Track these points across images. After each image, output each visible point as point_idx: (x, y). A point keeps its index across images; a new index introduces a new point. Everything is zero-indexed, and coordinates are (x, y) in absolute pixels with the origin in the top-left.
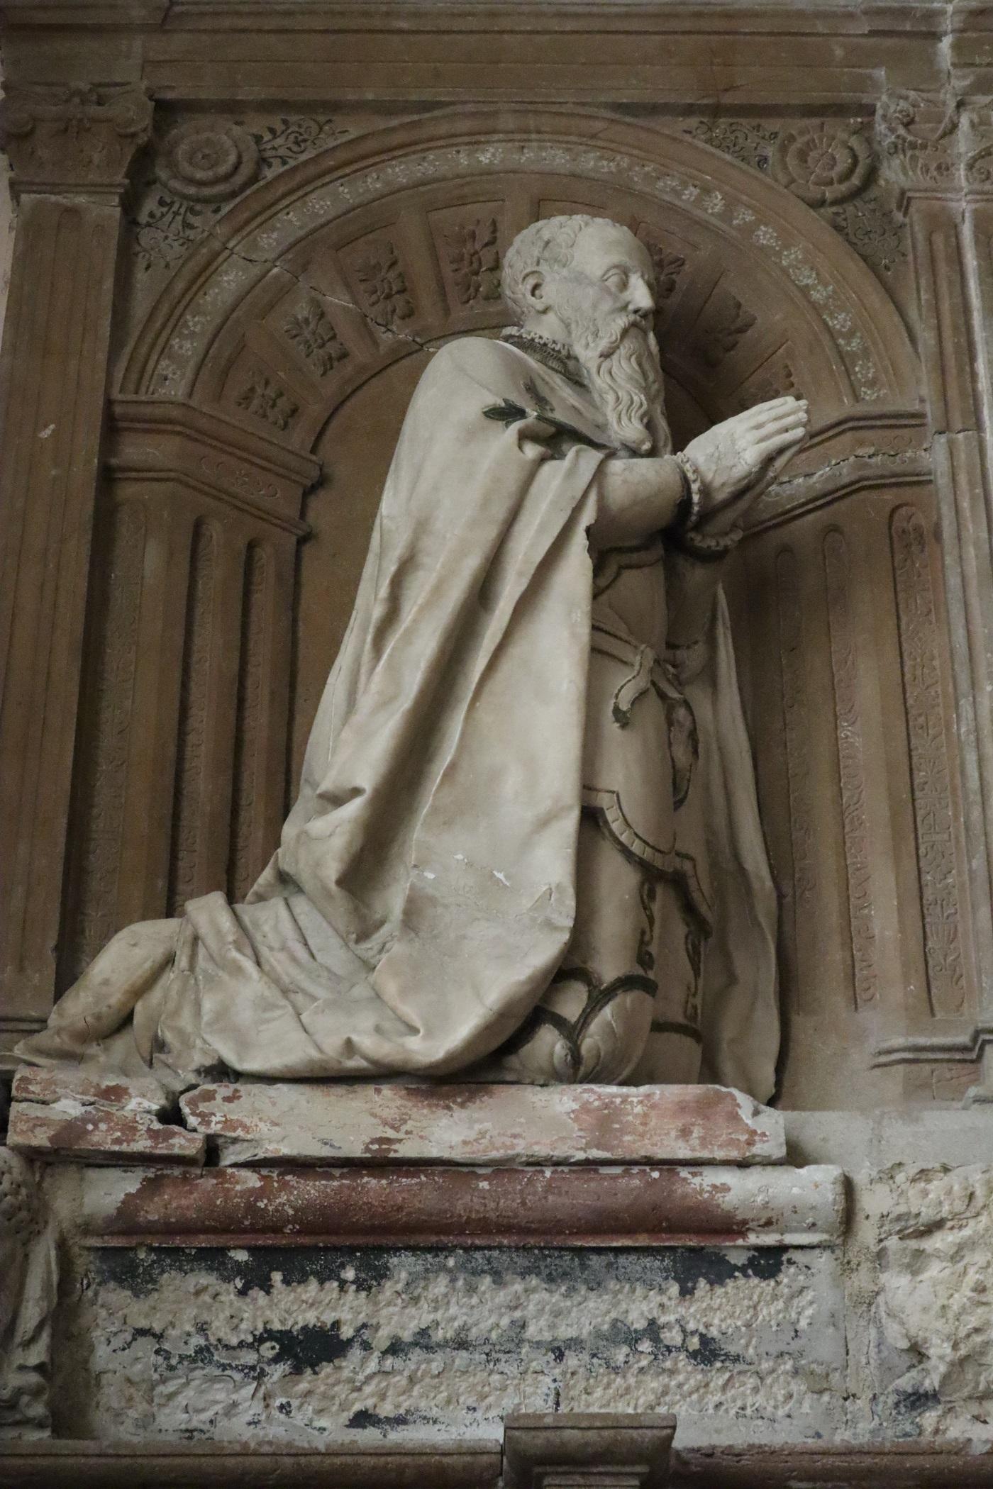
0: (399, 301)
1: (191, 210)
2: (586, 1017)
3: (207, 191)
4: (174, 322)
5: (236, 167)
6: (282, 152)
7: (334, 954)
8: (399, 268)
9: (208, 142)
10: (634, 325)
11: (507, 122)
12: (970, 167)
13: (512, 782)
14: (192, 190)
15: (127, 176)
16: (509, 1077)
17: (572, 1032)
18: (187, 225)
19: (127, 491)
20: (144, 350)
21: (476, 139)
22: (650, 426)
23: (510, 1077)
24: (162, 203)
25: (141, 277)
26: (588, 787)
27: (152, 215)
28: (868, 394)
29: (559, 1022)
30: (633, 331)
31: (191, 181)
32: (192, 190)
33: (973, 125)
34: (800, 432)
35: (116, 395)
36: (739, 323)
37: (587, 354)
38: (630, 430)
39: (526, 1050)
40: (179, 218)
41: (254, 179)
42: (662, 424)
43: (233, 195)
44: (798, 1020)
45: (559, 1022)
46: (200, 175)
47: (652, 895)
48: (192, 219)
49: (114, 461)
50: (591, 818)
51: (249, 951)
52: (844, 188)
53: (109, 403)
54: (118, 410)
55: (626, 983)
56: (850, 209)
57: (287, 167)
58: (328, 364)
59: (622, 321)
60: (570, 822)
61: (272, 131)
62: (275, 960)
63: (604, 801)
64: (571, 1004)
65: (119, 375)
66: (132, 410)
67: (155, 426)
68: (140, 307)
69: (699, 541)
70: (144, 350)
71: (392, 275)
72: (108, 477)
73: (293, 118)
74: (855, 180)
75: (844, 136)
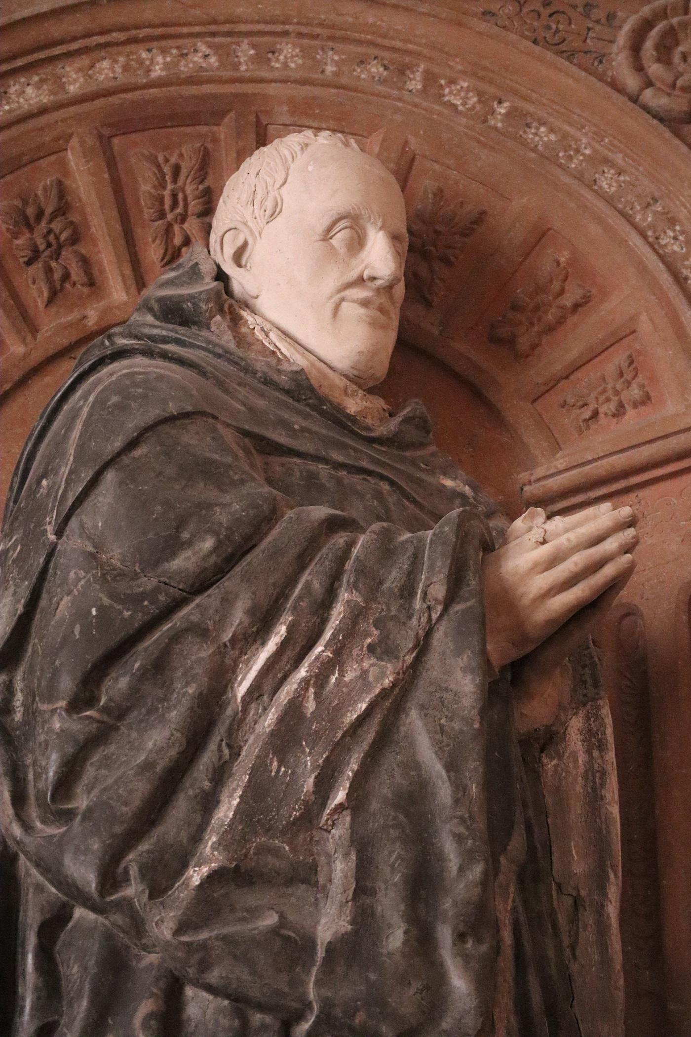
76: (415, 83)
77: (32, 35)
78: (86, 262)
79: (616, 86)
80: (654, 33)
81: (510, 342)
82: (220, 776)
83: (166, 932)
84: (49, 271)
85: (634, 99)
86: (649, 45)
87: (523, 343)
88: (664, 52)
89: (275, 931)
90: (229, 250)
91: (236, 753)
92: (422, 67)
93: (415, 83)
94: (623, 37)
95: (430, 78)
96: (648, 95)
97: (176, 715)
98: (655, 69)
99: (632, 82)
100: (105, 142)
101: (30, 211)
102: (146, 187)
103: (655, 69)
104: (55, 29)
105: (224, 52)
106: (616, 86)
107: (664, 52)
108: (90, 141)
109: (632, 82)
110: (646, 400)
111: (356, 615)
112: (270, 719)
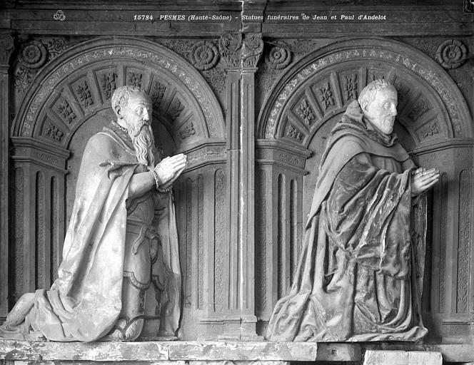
0: (89, 99)
1: (29, 71)
2: (126, 328)
3: (33, 66)
4: (27, 110)
5: (41, 55)
6: (54, 50)
7: (68, 307)
8: (89, 89)
9: (32, 49)
10: (145, 125)
11: (116, 41)
12: (244, 61)
13: (106, 272)
14: (29, 66)
15: (9, 64)
16: (110, 339)
17: (123, 331)
18: (28, 77)
19: (17, 165)
20: (19, 121)
21: (107, 47)
22: (148, 159)
23: (110, 339)
24: (21, 69)
25: (17, 94)
26: (125, 271)
27: (18, 73)
28: (212, 134)
29: (120, 329)
30: (144, 127)
31: (28, 63)
32: (29, 66)
33: (246, 46)
34: (184, 165)
35: (12, 137)
36: (180, 109)
37: (132, 136)
38: (143, 161)
39: (113, 334)
40: (26, 75)
41: (46, 61)
42: (152, 156)
43: (40, 67)
44: (186, 310)
45: (120, 329)
46: (30, 61)
47: (143, 294)
48: (31, 76)
49: (13, 157)
50: (126, 280)
51: (49, 308)
52: (211, 65)
53: (10, 140)
54: (13, 140)
55: (136, 318)
56: (212, 71)
57: (56, 57)
58: (71, 121)
59: (141, 125)
60: (120, 283)
61: (50, 43)
62: (56, 306)
63: (130, 275)
64: (123, 325)
65: (12, 131)
66: (16, 141)
67: (23, 145)
68: (18, 102)
69: (160, 190)
70: (19, 121)
71: (86, 92)
72: (12, 162)
73: (56, 39)
74: (214, 62)
75: (211, 46)
76: (398, 60)
77: (324, 50)
78: (333, 100)
79: (437, 62)
80: (446, 49)
81: (412, 118)
82: (365, 225)
83: (356, 256)
84: (326, 102)
85: (440, 64)
86: (445, 52)
87: (415, 119)
88: (447, 52)
89: (374, 256)
90: (364, 107)
91: (367, 221)
92: (399, 55)
93: (398, 60)
94: (440, 48)
95: (401, 58)
96: (443, 64)
97: (358, 213)
98: (446, 59)
99: (441, 61)
100: (338, 74)
101: (323, 90)
102: (345, 83)
103: (446, 59)
104: (328, 49)
105: (361, 52)
106: (437, 62)
107: (447, 52)
108: (335, 74)
109: (441, 61)
110: (438, 133)
111: (389, 193)
112: (374, 216)
